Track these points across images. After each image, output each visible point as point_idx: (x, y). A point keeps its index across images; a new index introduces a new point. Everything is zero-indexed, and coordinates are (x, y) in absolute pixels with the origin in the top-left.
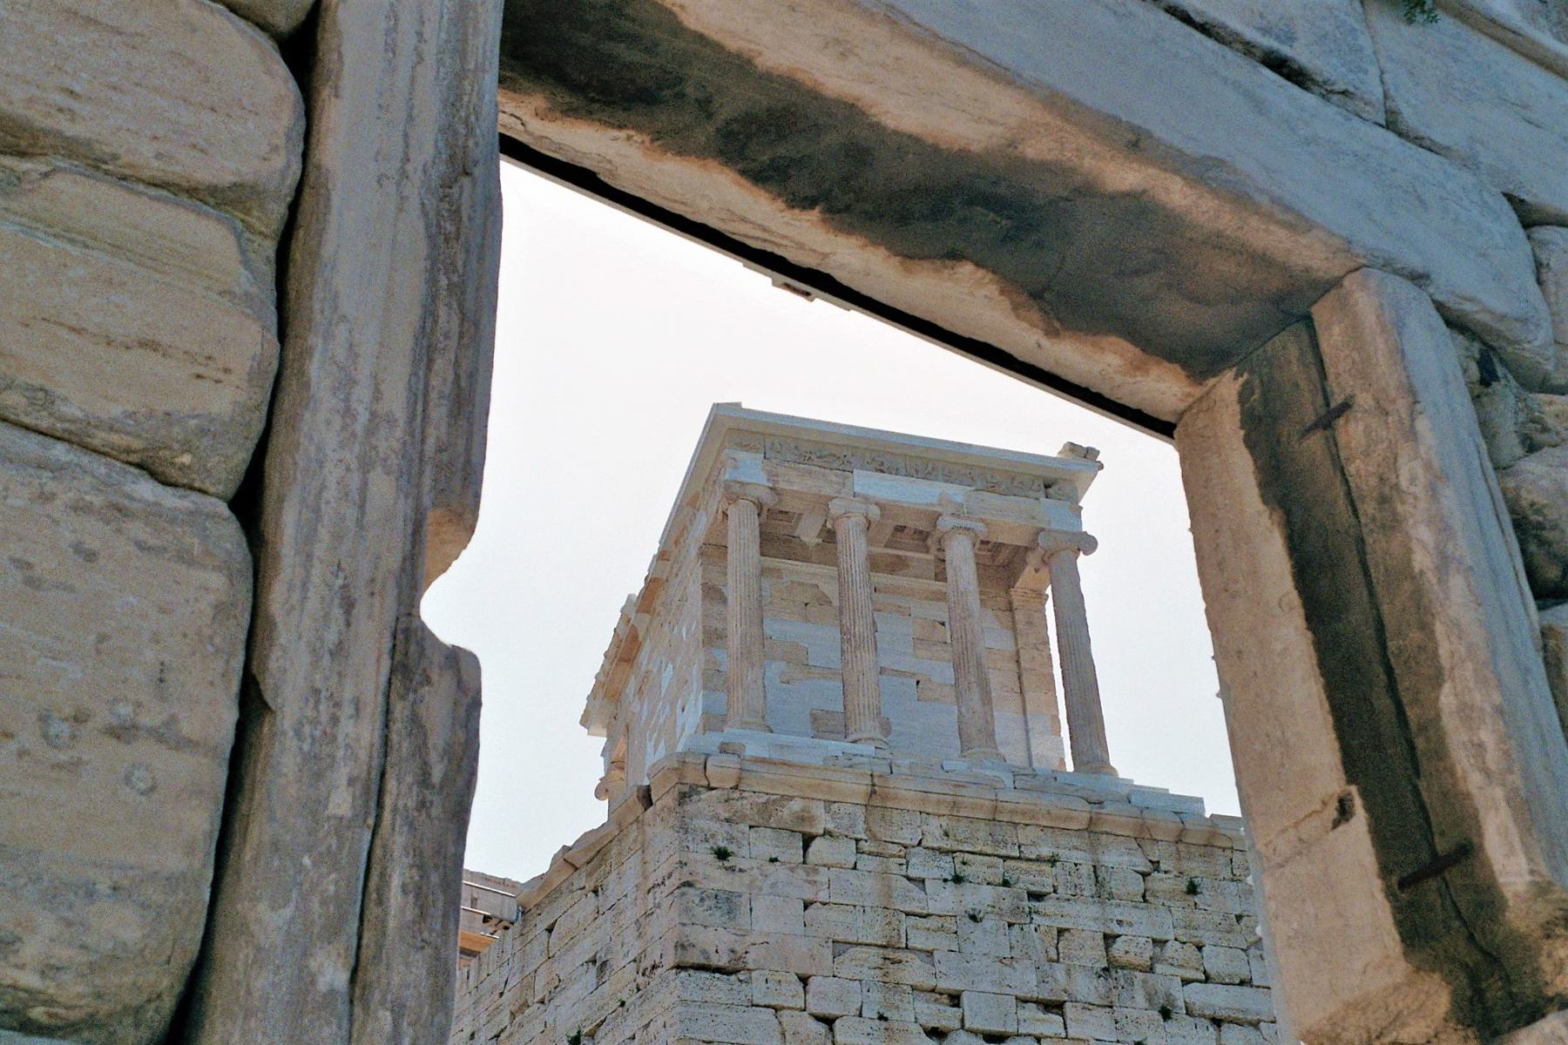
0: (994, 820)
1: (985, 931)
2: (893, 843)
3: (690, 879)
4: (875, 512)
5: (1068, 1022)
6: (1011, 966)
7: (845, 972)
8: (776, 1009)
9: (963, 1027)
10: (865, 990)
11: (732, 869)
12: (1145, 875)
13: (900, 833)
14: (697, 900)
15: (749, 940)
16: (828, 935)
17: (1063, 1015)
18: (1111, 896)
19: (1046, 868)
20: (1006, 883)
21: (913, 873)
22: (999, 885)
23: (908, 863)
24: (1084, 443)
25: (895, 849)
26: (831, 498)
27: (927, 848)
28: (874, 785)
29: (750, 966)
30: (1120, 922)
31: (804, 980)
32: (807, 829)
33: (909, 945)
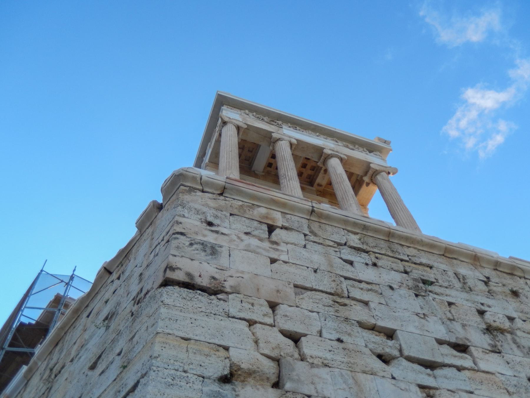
2: (328, 240)
3: (183, 231)
4: (294, 142)
6: (424, 318)
7: (304, 304)
8: (251, 323)
9: (402, 355)
10: (323, 319)
11: (217, 232)
13: (332, 236)
14: (187, 243)
15: (227, 273)
17: (471, 355)
19: (428, 269)
20: (406, 272)
21: (345, 257)
22: (402, 272)
23: (340, 252)
25: (331, 244)
26: (273, 133)
28: (313, 207)
29: (228, 290)
31: (273, 306)
32: (270, 222)
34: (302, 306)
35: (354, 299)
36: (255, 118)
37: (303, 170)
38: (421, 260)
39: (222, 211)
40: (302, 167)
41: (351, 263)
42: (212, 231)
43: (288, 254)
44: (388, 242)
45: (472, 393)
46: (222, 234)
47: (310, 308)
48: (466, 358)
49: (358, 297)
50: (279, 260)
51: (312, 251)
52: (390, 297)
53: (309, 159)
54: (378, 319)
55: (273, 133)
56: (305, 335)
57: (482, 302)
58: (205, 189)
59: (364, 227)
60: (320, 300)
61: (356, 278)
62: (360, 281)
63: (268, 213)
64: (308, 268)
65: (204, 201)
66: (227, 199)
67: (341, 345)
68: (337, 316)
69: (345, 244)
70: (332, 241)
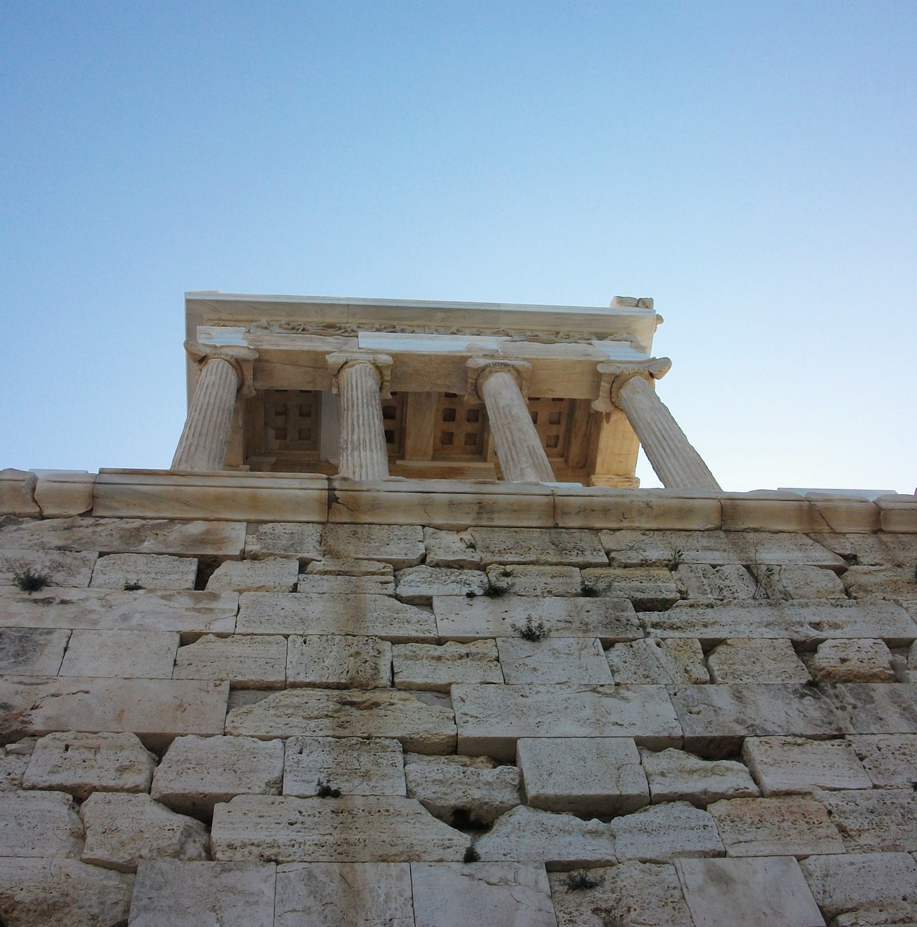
0: (556, 527)
1: (555, 653)
4: (385, 359)
5: (759, 768)
9: (523, 798)
11: (47, 602)
12: (840, 571)
16: (224, 675)
18: (787, 596)
21: (405, 591)
22: (577, 595)
24: (637, 294)
27: (437, 565)
30: (817, 626)
32: (209, 551)
33: (397, 680)
34: (243, 731)
35: (408, 688)
36: (286, 331)
37: (451, 426)
38: (646, 554)
39: (80, 552)
40: (445, 420)
41: (426, 603)
42: (35, 601)
43: (236, 616)
44: (553, 531)
45: (723, 854)
46: (63, 602)
47: (262, 733)
48: (728, 769)
49: (419, 680)
50: (207, 634)
51: (312, 595)
52: (521, 662)
53: (455, 395)
54: (466, 722)
55: (329, 353)
56: (227, 798)
57: (817, 619)
58: (46, 512)
59: (480, 507)
60: (298, 707)
61: (427, 635)
62: (440, 642)
63: (208, 532)
64: (287, 637)
65: (37, 537)
66: (102, 521)
67: (331, 803)
68: (339, 738)
69: (423, 560)
70: (379, 561)
